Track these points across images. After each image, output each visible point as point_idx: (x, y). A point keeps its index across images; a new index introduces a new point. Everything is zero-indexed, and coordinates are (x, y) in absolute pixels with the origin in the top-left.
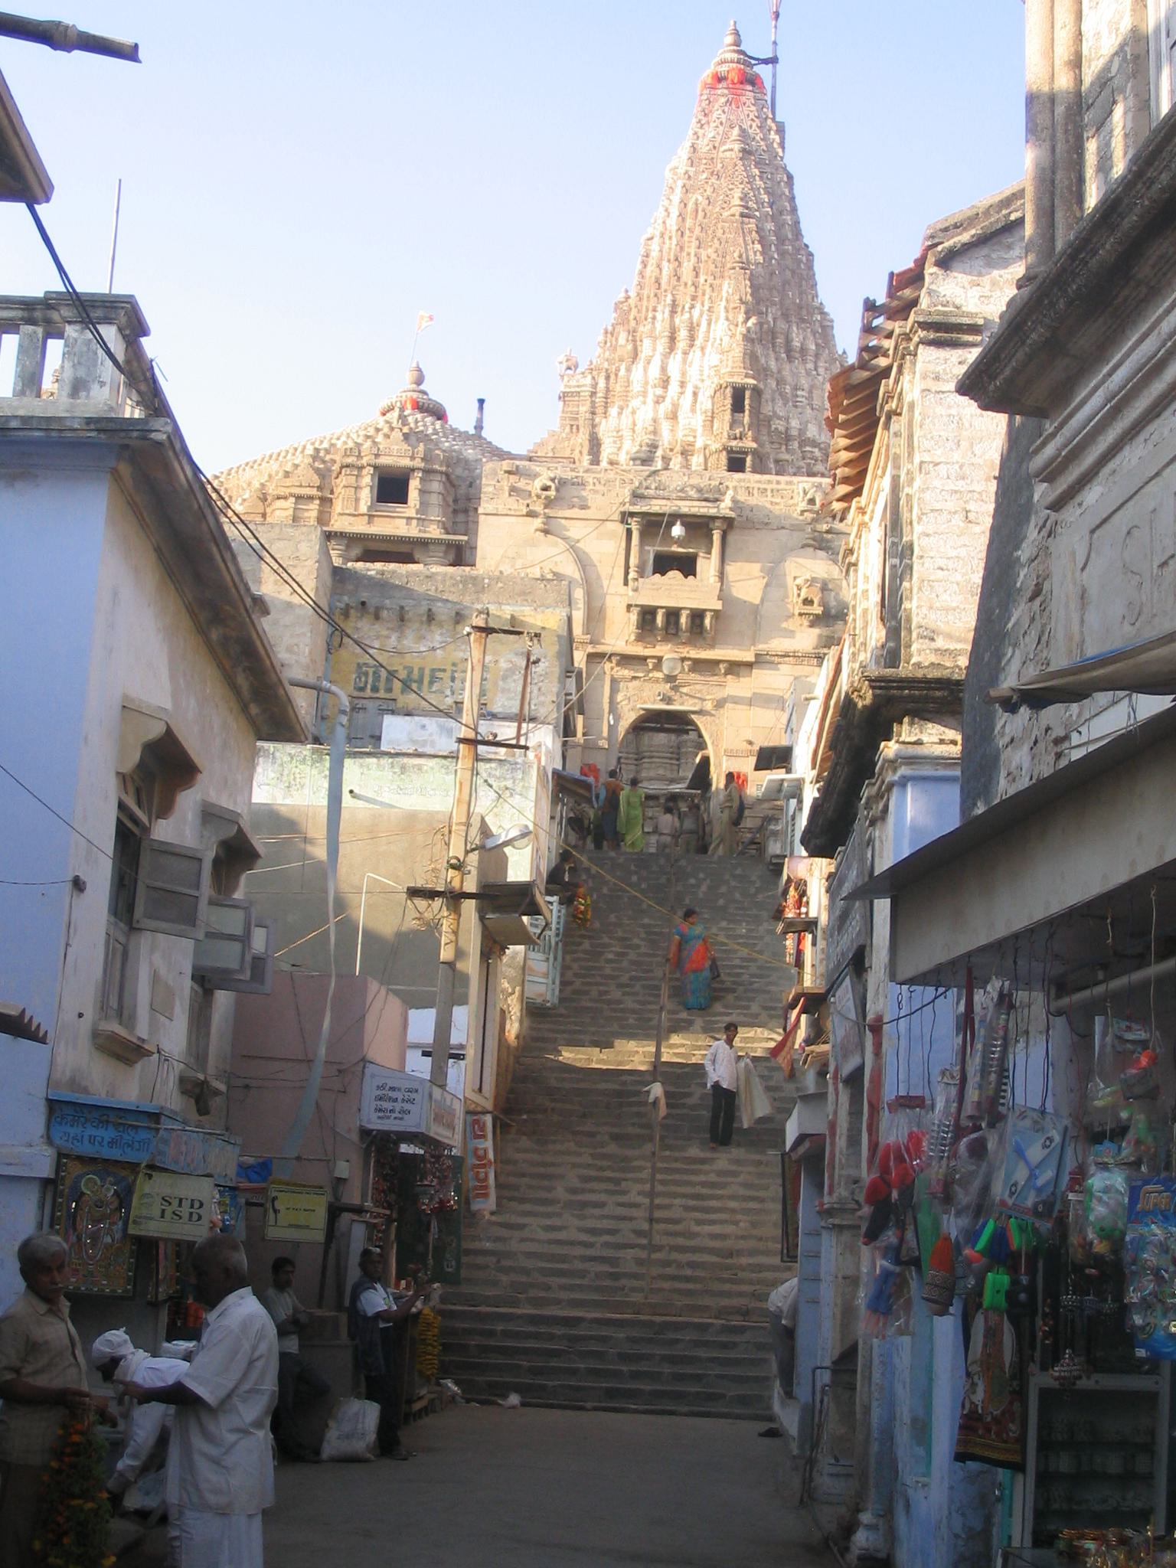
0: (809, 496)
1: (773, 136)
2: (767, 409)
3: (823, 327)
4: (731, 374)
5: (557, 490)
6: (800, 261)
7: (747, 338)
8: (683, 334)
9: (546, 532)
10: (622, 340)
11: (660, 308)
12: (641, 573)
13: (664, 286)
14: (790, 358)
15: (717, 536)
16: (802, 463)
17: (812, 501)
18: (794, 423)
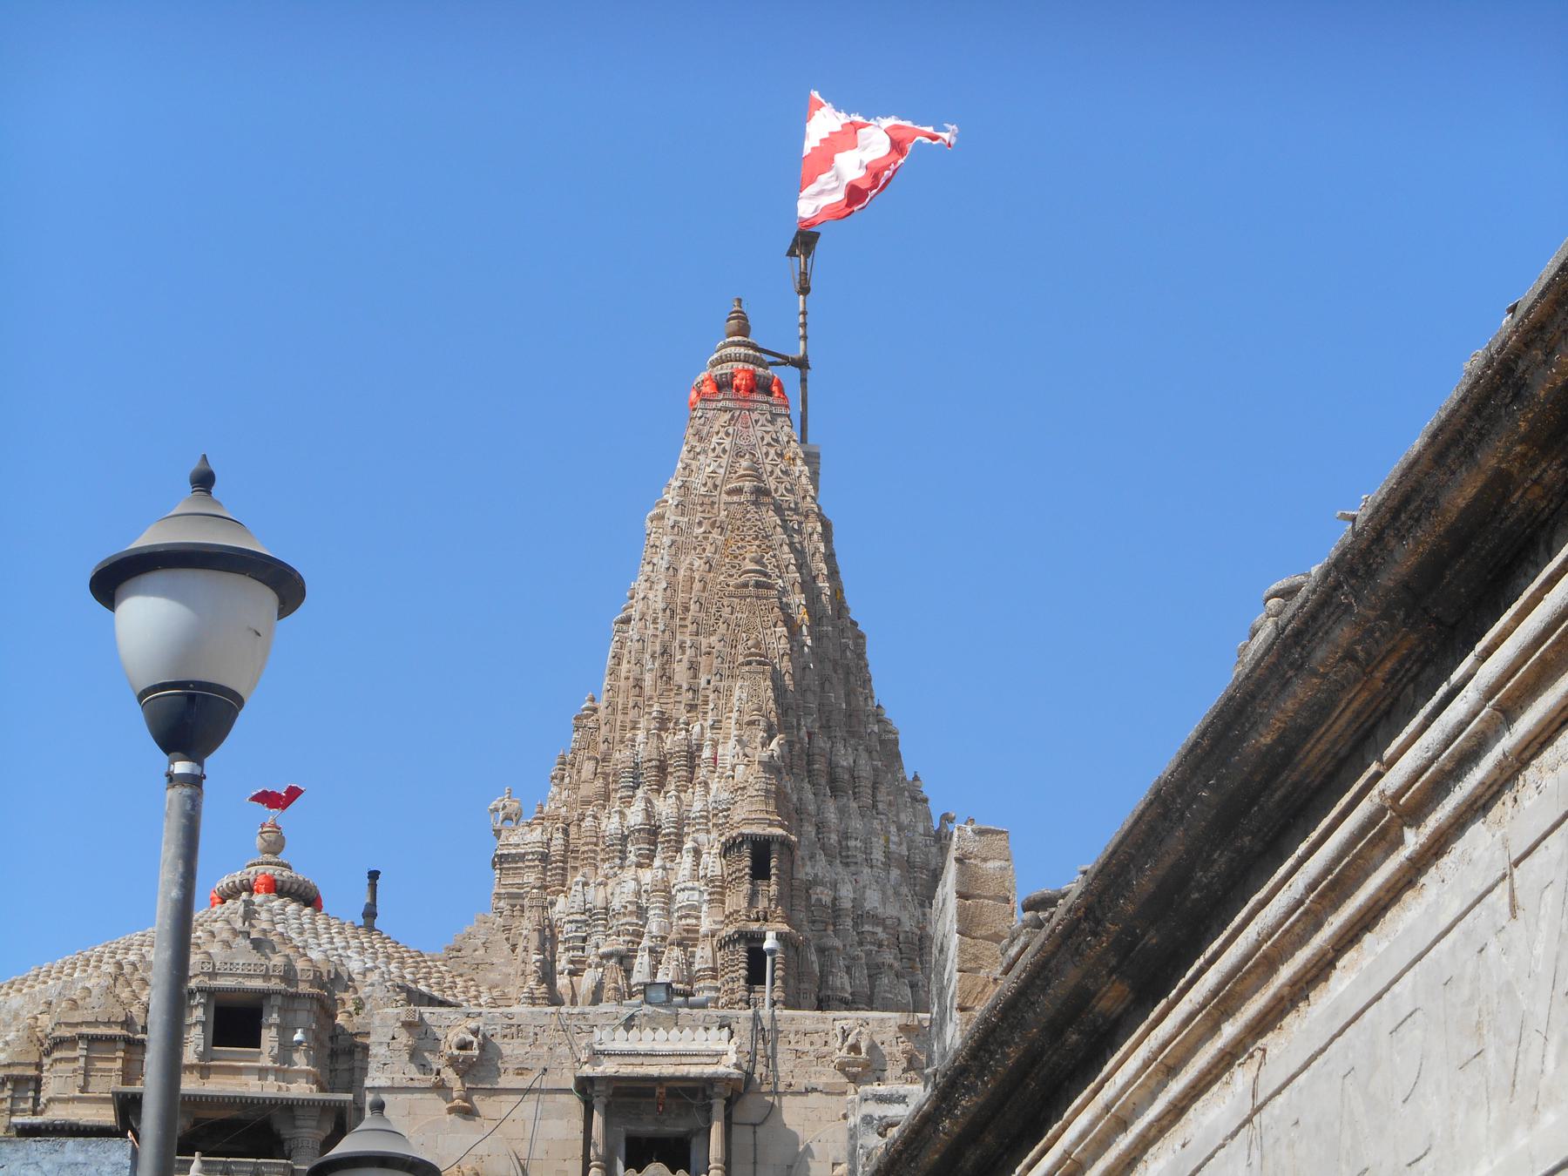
0: (851, 1040)
1: (800, 468)
2: (805, 872)
3: (882, 742)
4: (747, 821)
5: (482, 1047)
6: (847, 646)
7: (769, 766)
10: (588, 767)
11: (643, 724)
13: (648, 691)
14: (835, 790)
15: (718, 1107)
16: (859, 952)
17: (855, 1048)
18: (846, 892)
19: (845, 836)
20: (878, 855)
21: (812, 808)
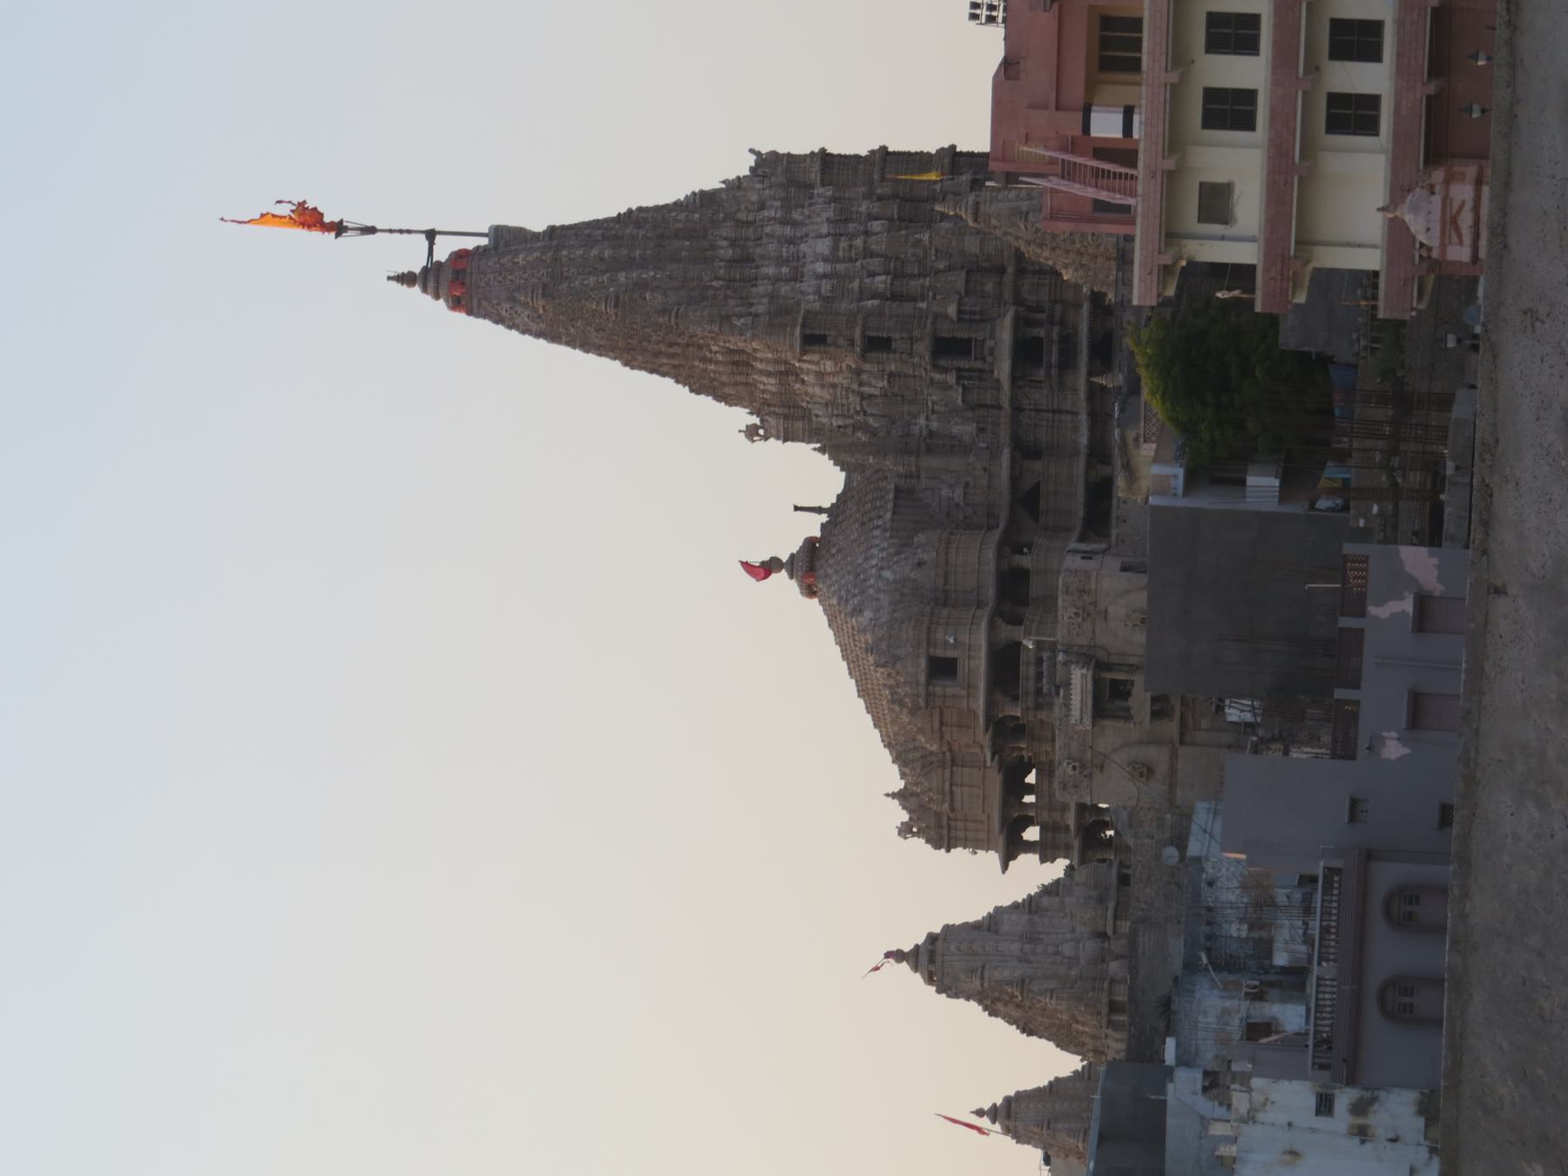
4: (791, 346)
8: (737, 358)
9: (1102, 768)
12: (1127, 716)
18: (820, 267)
19: (781, 261)
20: (788, 230)
21: (770, 288)
